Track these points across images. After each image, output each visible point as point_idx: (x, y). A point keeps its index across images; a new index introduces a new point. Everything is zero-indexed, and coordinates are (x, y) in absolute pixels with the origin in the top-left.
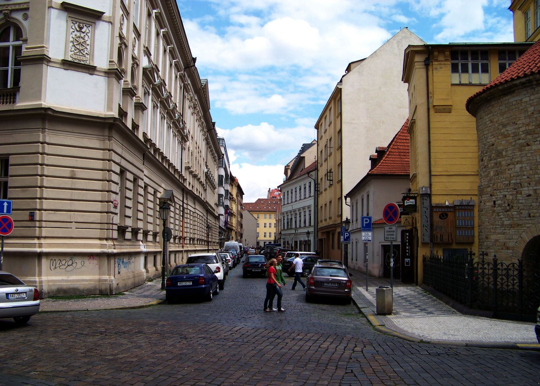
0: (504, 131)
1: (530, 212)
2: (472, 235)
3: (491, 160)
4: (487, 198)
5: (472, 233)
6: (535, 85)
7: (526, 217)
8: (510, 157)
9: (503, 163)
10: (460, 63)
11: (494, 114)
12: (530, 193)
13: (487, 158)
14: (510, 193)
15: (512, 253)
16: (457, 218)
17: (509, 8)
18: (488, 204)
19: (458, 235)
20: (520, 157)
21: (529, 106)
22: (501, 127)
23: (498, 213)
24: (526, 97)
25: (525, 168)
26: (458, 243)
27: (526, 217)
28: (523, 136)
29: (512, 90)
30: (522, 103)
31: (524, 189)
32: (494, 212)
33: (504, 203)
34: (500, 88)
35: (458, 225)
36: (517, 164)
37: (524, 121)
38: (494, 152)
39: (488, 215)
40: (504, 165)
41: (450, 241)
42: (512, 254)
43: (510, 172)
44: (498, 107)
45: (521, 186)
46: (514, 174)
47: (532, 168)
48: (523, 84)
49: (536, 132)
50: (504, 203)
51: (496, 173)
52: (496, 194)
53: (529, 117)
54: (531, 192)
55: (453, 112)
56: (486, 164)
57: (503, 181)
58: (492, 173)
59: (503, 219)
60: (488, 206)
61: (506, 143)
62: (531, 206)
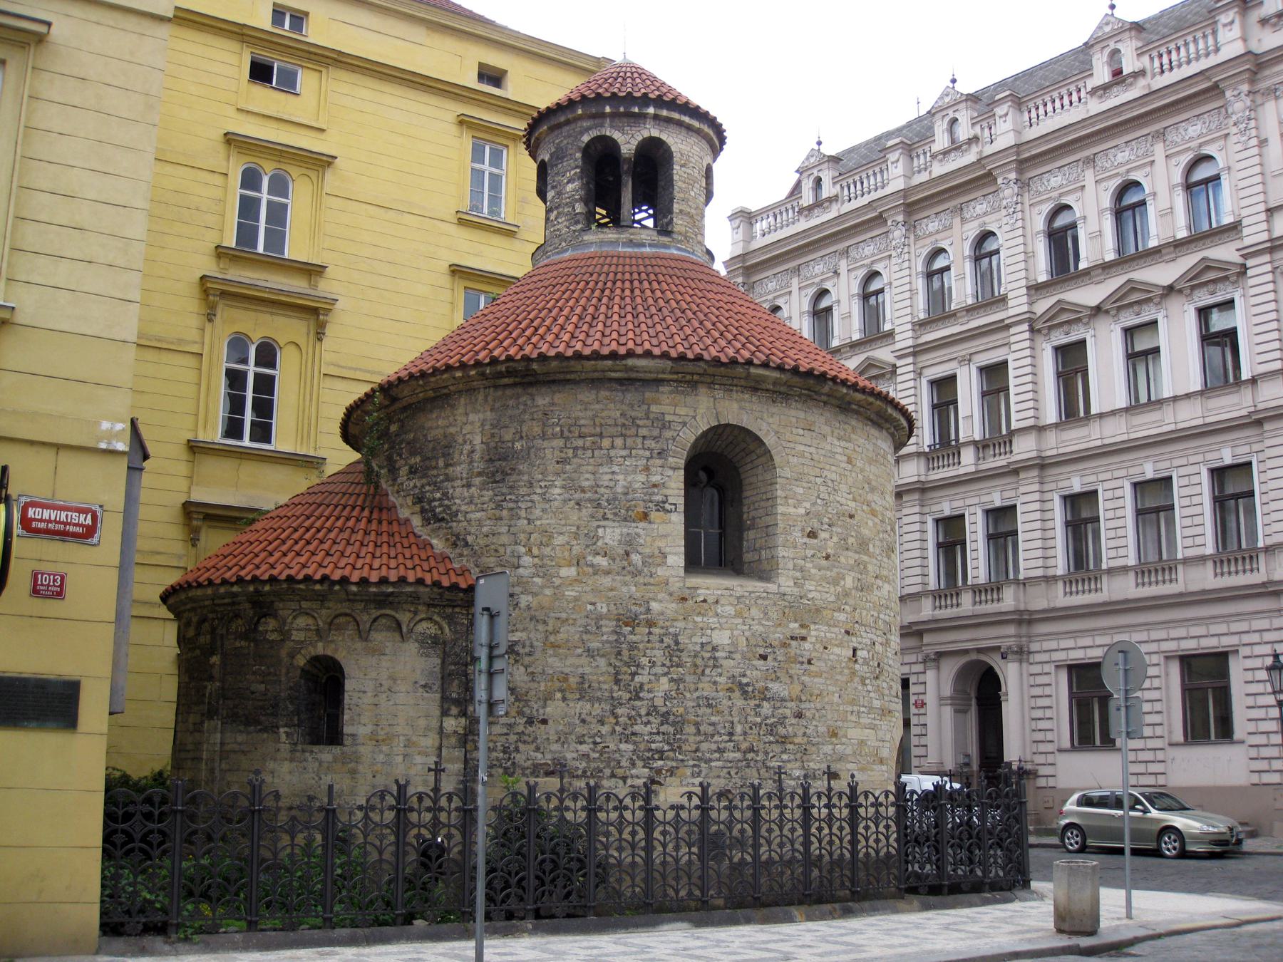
13: (835, 539)
18: (837, 650)
39: (839, 677)
59: (872, 695)
60: (839, 656)
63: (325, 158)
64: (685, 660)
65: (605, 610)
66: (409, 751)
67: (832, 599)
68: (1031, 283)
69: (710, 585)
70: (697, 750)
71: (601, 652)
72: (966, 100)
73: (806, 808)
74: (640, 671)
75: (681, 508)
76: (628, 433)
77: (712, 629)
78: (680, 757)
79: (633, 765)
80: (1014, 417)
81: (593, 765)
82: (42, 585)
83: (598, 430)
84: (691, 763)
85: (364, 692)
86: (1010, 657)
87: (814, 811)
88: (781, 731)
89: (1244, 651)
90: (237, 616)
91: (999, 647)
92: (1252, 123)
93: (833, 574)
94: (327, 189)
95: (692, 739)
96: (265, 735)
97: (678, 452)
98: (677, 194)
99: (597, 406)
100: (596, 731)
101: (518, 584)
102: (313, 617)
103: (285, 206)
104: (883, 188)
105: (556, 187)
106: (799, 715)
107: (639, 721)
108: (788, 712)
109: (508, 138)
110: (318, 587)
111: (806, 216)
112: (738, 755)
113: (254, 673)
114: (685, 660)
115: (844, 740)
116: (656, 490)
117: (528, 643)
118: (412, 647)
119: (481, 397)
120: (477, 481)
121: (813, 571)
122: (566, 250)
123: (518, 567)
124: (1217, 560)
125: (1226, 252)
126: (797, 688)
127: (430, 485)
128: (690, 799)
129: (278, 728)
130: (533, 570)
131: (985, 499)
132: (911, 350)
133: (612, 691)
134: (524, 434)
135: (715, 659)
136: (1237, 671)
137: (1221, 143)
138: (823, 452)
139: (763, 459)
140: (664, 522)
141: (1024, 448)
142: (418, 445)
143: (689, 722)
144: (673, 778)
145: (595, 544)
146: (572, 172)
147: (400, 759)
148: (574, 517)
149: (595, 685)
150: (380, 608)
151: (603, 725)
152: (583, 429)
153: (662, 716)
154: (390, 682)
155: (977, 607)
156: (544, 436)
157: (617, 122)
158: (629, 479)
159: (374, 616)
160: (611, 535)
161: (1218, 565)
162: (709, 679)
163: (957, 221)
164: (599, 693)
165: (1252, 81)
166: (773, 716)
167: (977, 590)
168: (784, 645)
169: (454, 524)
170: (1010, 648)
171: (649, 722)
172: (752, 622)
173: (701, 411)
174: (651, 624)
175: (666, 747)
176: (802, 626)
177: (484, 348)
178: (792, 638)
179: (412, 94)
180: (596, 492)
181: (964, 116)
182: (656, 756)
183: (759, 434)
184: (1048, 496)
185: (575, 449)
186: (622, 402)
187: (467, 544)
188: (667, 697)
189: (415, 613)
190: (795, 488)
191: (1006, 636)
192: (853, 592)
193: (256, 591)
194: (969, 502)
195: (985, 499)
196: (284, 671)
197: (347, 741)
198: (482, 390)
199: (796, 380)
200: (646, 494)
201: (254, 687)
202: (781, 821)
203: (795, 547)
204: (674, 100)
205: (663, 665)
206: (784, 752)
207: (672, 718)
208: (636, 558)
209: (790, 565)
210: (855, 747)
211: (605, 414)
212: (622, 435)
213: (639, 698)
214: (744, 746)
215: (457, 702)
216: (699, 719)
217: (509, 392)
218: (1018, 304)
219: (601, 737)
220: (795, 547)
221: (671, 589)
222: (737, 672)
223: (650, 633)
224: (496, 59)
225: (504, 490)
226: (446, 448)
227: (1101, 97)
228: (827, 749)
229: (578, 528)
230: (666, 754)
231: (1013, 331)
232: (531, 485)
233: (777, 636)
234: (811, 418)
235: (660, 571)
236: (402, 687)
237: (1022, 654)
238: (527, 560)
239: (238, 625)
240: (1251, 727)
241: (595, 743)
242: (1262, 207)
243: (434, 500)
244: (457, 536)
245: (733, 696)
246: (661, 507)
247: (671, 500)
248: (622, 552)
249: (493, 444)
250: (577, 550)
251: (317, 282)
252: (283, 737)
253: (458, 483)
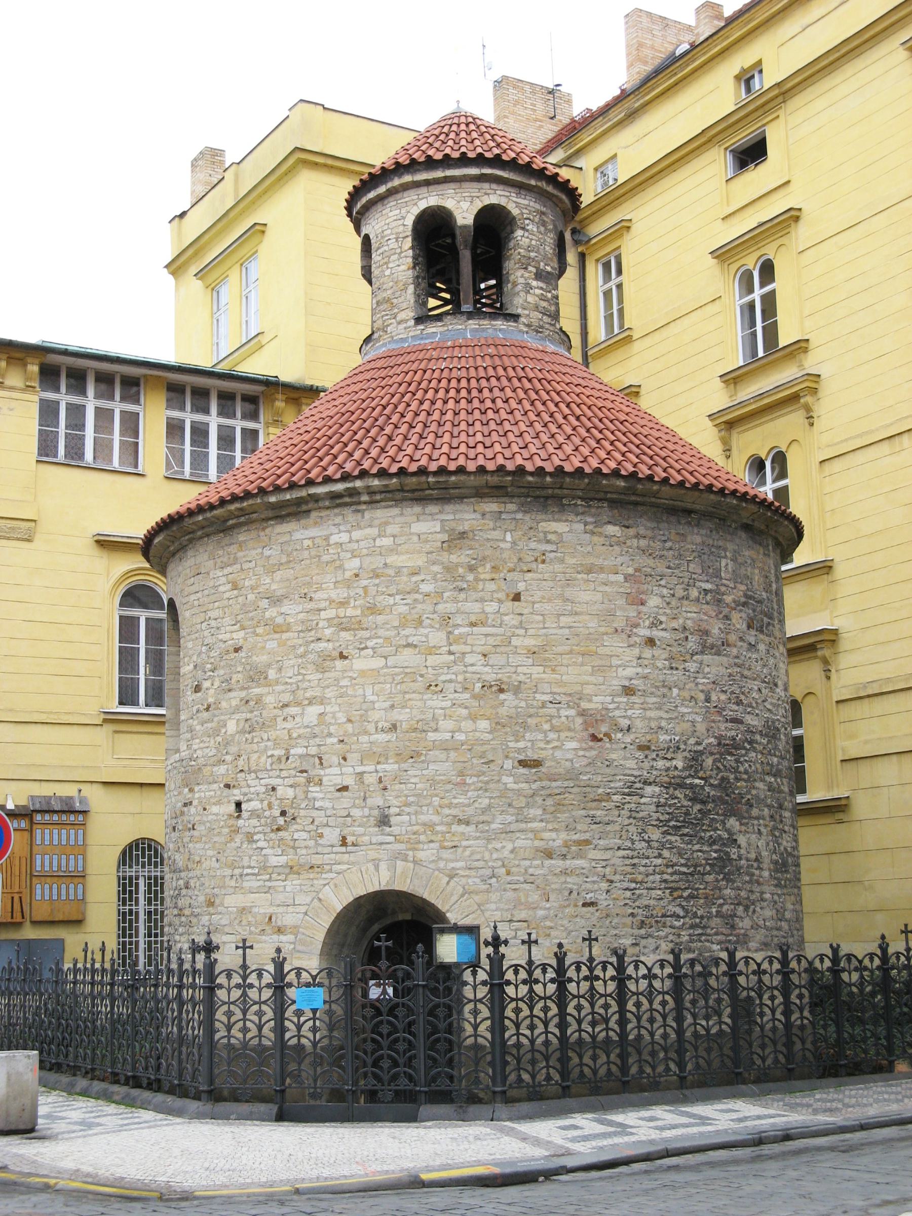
0: (274, 615)
1: (345, 832)
2: (80, 897)
3: (230, 690)
4: (212, 793)
5: (80, 892)
6: (365, 503)
7: (332, 846)
8: (291, 684)
9: (269, 700)
10: (64, 398)
11: (245, 566)
12: (345, 784)
13: (217, 684)
14: (290, 781)
15: (294, 943)
16: (35, 848)
17: (166, 267)
18: (215, 809)
19: (39, 897)
20: (318, 685)
21: (349, 555)
22: (264, 603)
23: (250, 838)
24: (340, 532)
25: (334, 717)
26: (35, 923)
27: (332, 846)
28: (328, 632)
29: (304, 508)
30: (329, 545)
31: (328, 771)
32: (237, 831)
33: (270, 806)
34: (273, 499)
35: (38, 868)
36: (310, 704)
37: (333, 594)
38: (239, 669)
39: (216, 839)
40: (271, 706)
41: (18, 919)
42: (292, 946)
43: (288, 725)
44: (260, 550)
45: (321, 764)
46: (302, 731)
47: (353, 719)
48: (334, 496)
49: (364, 626)
50: (270, 806)
51: (247, 726)
52: (243, 783)
53: (348, 583)
54: (349, 781)
55: (38, 538)
56: (211, 700)
57: (266, 748)
58: (232, 727)
59: (264, 851)
60: (217, 815)
61: (279, 645)
62: (348, 816)
67: (214, 751)
73: (561, 981)
93: (213, 725)
138: (206, 592)
176: (191, 790)
178: (185, 805)
179: (859, 63)
202: (531, 999)
210: (233, 916)
234: (199, 559)
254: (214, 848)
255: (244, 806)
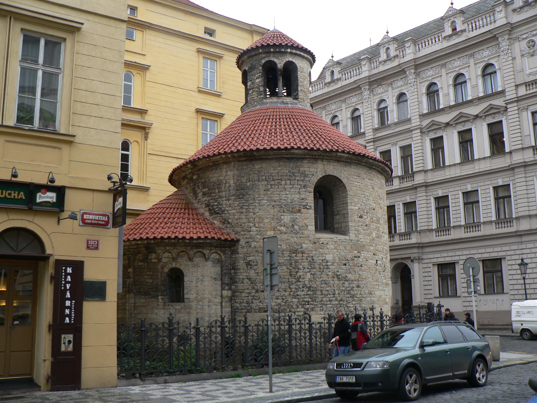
18: (371, 261)
39: (371, 271)
59: (383, 278)
60: (371, 263)
63: (146, 66)
64: (316, 266)
65: (285, 248)
66: (210, 304)
67: (368, 241)
68: (421, 114)
69: (325, 237)
70: (322, 301)
71: (284, 264)
72: (393, 40)
74: (299, 271)
75: (313, 208)
76: (292, 178)
77: (326, 254)
78: (315, 304)
79: (298, 307)
80: (414, 166)
81: (282, 307)
82: (90, 245)
83: (280, 177)
84: (320, 306)
85: (192, 282)
86: (414, 261)
87: (368, 323)
88: (352, 292)
89: (508, 258)
90: (139, 253)
91: (410, 257)
92: (510, 51)
93: (369, 232)
94: (147, 79)
95: (320, 296)
96: (153, 299)
97: (311, 186)
98: (300, 83)
99: (279, 168)
100: (283, 294)
101: (251, 238)
102: (170, 252)
103: (131, 86)
104: (359, 75)
105: (251, 80)
106: (358, 287)
107: (300, 290)
108: (354, 285)
109: (216, 57)
110: (173, 241)
111: (328, 86)
112: (337, 302)
113: (147, 275)
114: (316, 266)
115: (374, 295)
116: (303, 201)
117: (255, 261)
118: (209, 264)
119: (232, 164)
120: (232, 198)
121: (362, 231)
122: (257, 106)
123: (250, 231)
124: (497, 222)
125: (499, 102)
126: (358, 276)
127: (212, 200)
128: (325, 320)
129: (158, 296)
130: (256, 233)
131: (403, 199)
132: (372, 140)
133: (289, 279)
134: (251, 180)
135: (327, 265)
136: (505, 265)
137: (497, 59)
138: (364, 185)
139: (342, 188)
140: (306, 213)
141: (419, 179)
142: (206, 184)
143: (318, 290)
144: (313, 312)
145: (280, 222)
146: (258, 75)
147: (207, 307)
148: (272, 211)
149: (282, 277)
150: (198, 249)
151: (286, 292)
152: (274, 177)
153: (308, 288)
154: (202, 277)
155: (401, 242)
156: (259, 180)
157: (276, 55)
158: (293, 196)
159: (195, 252)
160: (287, 218)
161: (497, 225)
162: (325, 273)
163: (390, 89)
164: (284, 280)
165: (509, 34)
166: (349, 287)
167: (401, 235)
168: (352, 260)
169: (224, 215)
170: (414, 258)
171: (303, 291)
172: (340, 251)
173: (319, 170)
174: (303, 253)
175: (310, 300)
176: (358, 252)
177: (227, 147)
178: (355, 257)
180: (280, 202)
181: (393, 47)
182: (306, 304)
183: (341, 178)
184: (429, 198)
185: (271, 185)
186: (289, 167)
187: (229, 223)
188: (310, 281)
189: (211, 250)
190: (354, 199)
191: (414, 253)
192: (376, 238)
193: (148, 243)
194: (397, 200)
195: (403, 199)
196: (159, 274)
197: (186, 301)
198: (233, 163)
199: (354, 157)
200: (299, 202)
201: (147, 281)
203: (355, 222)
204: (298, 46)
205: (308, 268)
206: (354, 300)
207: (312, 288)
208: (296, 227)
209: (354, 229)
211: (283, 171)
212: (289, 179)
213: (300, 282)
214: (339, 299)
215: (227, 284)
216: (322, 289)
217: (244, 163)
218: (416, 122)
219: (285, 296)
220: (355, 222)
221: (310, 239)
222: (336, 270)
223: (303, 256)
224: (211, 25)
225: (244, 202)
226: (219, 184)
227: (448, 40)
228: (369, 299)
229: (274, 216)
230: (310, 303)
231: (413, 132)
232: (254, 199)
233: (349, 257)
235: (306, 232)
236: (206, 279)
237: (420, 259)
238: (254, 229)
239: (140, 256)
240: (511, 287)
241: (283, 299)
242: (514, 84)
243: (215, 205)
244: (225, 219)
245: (334, 279)
246: (305, 207)
247: (309, 204)
248: (291, 225)
249: (238, 184)
250: (274, 224)
251: (144, 116)
252: (160, 300)
253: (224, 199)
254: (371, 274)
255: (378, 262)
